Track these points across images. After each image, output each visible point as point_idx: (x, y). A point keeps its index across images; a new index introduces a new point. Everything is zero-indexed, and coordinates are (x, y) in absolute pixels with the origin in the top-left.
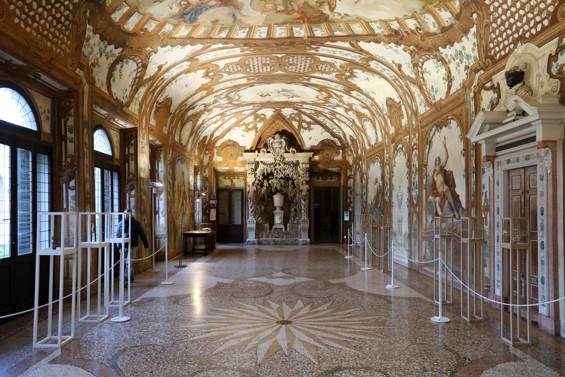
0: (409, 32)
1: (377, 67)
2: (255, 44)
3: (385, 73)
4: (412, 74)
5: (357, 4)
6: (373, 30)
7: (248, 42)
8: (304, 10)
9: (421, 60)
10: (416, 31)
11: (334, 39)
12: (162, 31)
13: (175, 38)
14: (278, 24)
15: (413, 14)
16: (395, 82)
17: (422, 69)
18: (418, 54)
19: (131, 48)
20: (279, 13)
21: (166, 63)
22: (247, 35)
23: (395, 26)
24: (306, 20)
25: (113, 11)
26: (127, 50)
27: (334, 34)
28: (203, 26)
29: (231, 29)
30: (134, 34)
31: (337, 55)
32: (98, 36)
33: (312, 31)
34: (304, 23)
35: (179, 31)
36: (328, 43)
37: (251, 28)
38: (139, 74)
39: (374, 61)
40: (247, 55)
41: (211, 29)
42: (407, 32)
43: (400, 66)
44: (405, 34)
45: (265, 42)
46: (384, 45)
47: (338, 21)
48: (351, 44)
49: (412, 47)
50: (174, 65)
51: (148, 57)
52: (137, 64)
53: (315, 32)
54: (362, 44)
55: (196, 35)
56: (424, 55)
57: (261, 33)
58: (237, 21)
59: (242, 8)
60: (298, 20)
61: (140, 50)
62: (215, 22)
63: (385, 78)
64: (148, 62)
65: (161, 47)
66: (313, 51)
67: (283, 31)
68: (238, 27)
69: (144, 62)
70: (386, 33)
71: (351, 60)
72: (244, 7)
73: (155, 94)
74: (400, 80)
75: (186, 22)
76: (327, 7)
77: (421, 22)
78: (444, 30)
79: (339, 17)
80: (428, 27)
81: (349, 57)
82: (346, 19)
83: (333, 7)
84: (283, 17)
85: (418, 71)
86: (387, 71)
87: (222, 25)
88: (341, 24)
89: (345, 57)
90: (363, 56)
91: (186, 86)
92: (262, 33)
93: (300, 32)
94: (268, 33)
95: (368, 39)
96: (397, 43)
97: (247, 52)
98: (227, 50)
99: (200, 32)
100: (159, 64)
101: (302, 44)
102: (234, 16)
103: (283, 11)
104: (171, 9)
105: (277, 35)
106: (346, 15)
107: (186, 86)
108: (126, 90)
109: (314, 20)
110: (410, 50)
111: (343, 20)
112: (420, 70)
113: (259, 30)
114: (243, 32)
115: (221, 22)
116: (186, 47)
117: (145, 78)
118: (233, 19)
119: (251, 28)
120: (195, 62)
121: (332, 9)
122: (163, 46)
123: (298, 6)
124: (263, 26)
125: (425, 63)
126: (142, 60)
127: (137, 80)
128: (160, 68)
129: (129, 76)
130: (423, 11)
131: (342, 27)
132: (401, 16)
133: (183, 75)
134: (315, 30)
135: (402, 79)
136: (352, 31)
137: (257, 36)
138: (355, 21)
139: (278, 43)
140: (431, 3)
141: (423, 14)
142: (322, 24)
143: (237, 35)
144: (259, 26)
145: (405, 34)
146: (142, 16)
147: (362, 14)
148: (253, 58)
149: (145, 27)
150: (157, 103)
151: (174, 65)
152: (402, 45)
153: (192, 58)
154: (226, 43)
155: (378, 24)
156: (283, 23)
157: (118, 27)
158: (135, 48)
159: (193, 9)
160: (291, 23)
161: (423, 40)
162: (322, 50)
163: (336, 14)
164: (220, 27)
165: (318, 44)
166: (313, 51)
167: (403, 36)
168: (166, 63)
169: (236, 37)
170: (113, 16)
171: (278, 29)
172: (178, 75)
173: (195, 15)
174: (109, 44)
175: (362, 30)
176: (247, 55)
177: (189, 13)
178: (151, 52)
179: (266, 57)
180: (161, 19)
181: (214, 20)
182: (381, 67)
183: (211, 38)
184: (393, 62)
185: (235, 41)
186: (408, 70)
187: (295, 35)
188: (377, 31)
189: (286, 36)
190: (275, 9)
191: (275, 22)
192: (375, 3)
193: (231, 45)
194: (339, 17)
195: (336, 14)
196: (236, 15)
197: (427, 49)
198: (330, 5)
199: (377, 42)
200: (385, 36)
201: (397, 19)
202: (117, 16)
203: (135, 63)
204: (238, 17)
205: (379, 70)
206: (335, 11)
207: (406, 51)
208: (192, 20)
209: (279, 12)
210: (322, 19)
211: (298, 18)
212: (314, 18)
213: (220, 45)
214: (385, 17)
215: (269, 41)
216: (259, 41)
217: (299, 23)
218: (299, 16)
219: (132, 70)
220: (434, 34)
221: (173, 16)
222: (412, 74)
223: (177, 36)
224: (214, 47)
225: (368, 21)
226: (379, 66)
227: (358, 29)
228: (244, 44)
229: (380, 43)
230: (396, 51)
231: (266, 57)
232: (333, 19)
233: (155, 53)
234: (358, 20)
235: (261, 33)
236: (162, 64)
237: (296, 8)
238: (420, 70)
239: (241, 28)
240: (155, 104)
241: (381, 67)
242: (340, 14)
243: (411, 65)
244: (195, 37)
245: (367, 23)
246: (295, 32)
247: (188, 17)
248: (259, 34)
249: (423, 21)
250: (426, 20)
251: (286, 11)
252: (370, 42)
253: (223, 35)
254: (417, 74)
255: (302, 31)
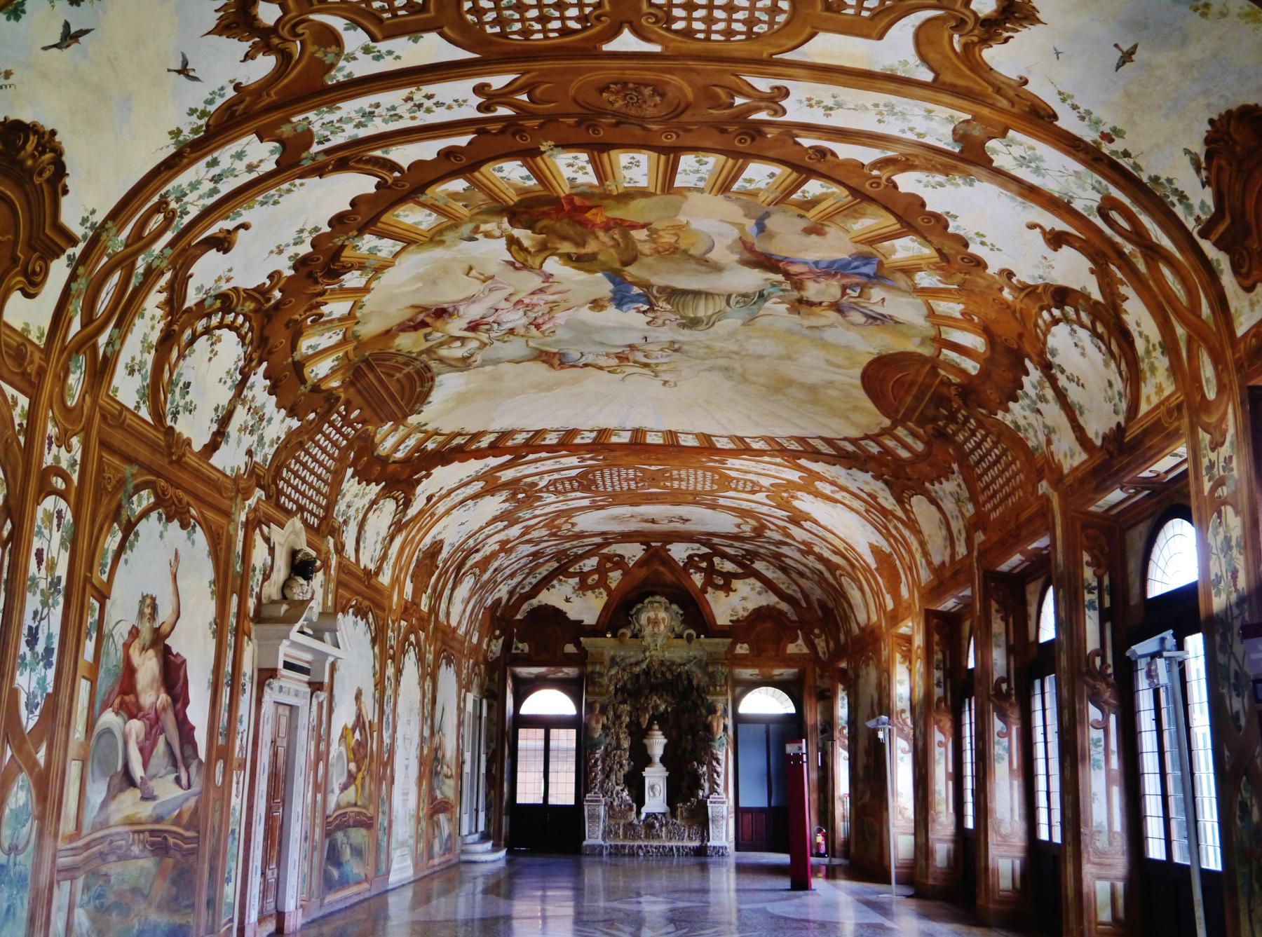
0: (320, 299)
1: (239, 156)
2: (723, 131)
3: (197, 171)
4: (199, 289)
5: (466, 266)
6: (381, 235)
7: (744, 138)
8: (579, 228)
9: (240, 319)
10: (314, 311)
11: (455, 164)
12: (942, 286)
13: (939, 251)
14: (643, 193)
15: (355, 318)
16: (156, 209)
17: (220, 327)
18: (256, 311)
19: (1020, 336)
20: (642, 222)
21: (1032, 226)
22: (742, 169)
23: (353, 279)
24: (566, 207)
25: (963, 372)
26: (1027, 347)
27: (468, 180)
28: (852, 235)
29: (784, 197)
30: (986, 331)
31: (392, 98)
32: (1011, 404)
33: (536, 173)
34: (570, 198)
35: (912, 258)
36: (462, 141)
37: (725, 188)
38: (1084, 316)
39: (270, 166)
40: (770, 62)
41: (838, 219)
42: (323, 293)
43: (223, 243)
44: (319, 288)
45: (688, 140)
46: (316, 229)
47: (480, 217)
48: (392, 166)
49: (277, 294)
50: (1031, 193)
51: (1029, 291)
52: (1056, 322)
53: (525, 172)
54: (365, 184)
55: (887, 222)
56: (251, 329)
57: (697, 171)
58: (760, 214)
59: (735, 241)
60: (587, 203)
61: (1018, 315)
62: (815, 230)
63: (171, 166)
64: (1046, 286)
65: (985, 267)
66: (498, 82)
67: (627, 173)
68: (762, 197)
69: (1047, 300)
70: (346, 253)
71: (331, 104)
72: (729, 242)
73: (1165, 242)
74: (169, 236)
75: (880, 264)
76: (526, 243)
77: (329, 325)
78: (298, 367)
79: (483, 227)
80: (314, 334)
81: (349, 108)
82: (466, 229)
83: (514, 248)
84: (633, 211)
85: (209, 316)
86: (207, 186)
87: (801, 216)
88: (466, 212)
89: (365, 102)
90: (315, 148)
91: (1127, 57)
92: (694, 169)
93: (571, 169)
94: (672, 170)
95: (363, 208)
96: (301, 264)
97: (763, 84)
98: (838, 120)
99: (872, 221)
100: (1044, 249)
101: (551, 118)
102: (761, 228)
103: (635, 226)
104: (883, 300)
105: (644, 157)
106: (472, 239)
107: (1127, 57)
108: (1110, 384)
109: (546, 208)
110: (272, 288)
111: (471, 226)
112: (215, 320)
113: (701, 179)
114: (750, 181)
115: (803, 224)
116: (939, 211)
117: (1097, 295)
118: (767, 222)
119: (725, 188)
120: (977, 131)
121: (513, 242)
122: (979, 263)
123: (597, 238)
124: (689, 189)
125: (234, 334)
126: (1042, 309)
127: (1100, 329)
128: (1056, 240)
129: (1083, 354)
130: (349, 334)
131: (458, 206)
132: (366, 298)
133: (1067, 121)
134: (528, 178)
135: (172, 244)
136: (424, 205)
137: (712, 160)
138: (441, 232)
139: (638, 132)
140: (355, 349)
141: (344, 334)
142: (516, 199)
143: (772, 175)
144: (701, 190)
145: (319, 288)
146: (942, 328)
147: (438, 253)
148: (750, 34)
149: (959, 316)
150: (1204, 234)
151: (1031, 193)
152: (292, 272)
153: (969, 157)
154: (822, 153)
155: (384, 254)
156: (628, 196)
157: (988, 363)
158: (1015, 327)
159: (844, 276)
160: (607, 196)
161: (287, 325)
162: (458, 99)
163: (497, 233)
164: (813, 212)
165: (494, 128)
166: (498, 82)
167: (316, 282)
168: (1032, 226)
169: (778, 170)
170: (974, 372)
171: (643, 182)
172: (1071, 144)
173: (849, 263)
174: (1021, 387)
175: (402, 219)
176: (765, 64)
177: (860, 274)
178: (1014, 288)
179: (688, 33)
180: (919, 301)
181: (814, 237)
182: (231, 172)
183: (854, 192)
184: (245, 226)
185: (788, 152)
186: (208, 273)
187: (584, 157)
188: (368, 242)
189: (613, 153)
190: (653, 234)
191: (654, 199)
192: (434, 283)
193: (807, 142)
194: (483, 227)
195: (497, 233)
196: (755, 230)
197: (266, 333)
198: (522, 248)
199: (338, 221)
200: (343, 247)
201: (366, 290)
202: (972, 367)
203: (1054, 329)
204: (750, 225)
205: (225, 155)
206: (503, 241)
207: (271, 277)
208: (866, 258)
209: (643, 226)
210: (525, 211)
211: (590, 208)
212: (546, 215)
213: (845, 151)
214: (388, 277)
215: (671, 140)
216: (707, 144)
217: (583, 195)
218: (589, 215)
219: (1071, 342)
220: (294, 346)
221: (891, 288)
222: (199, 289)
223: (927, 251)
224: (867, 155)
225: (412, 248)
226: (240, 166)
227: (412, 216)
228: (763, 135)
229: (330, 224)
230: (280, 252)
231: (688, 33)
232: (497, 219)
233: (1010, 274)
234: (435, 238)
235: (697, 171)
236: (1041, 237)
237: (601, 234)
238: (215, 320)
239: (754, 194)
240: (1207, 246)
241: (231, 172)
242: (488, 235)
243: (225, 287)
244: (892, 220)
245: (409, 240)
246: (589, 168)
247: (867, 270)
248: (704, 168)
249: (329, 330)
250: (327, 335)
251: (626, 226)
252: (353, 203)
253: (814, 187)
254: (202, 310)
255: (567, 173)
